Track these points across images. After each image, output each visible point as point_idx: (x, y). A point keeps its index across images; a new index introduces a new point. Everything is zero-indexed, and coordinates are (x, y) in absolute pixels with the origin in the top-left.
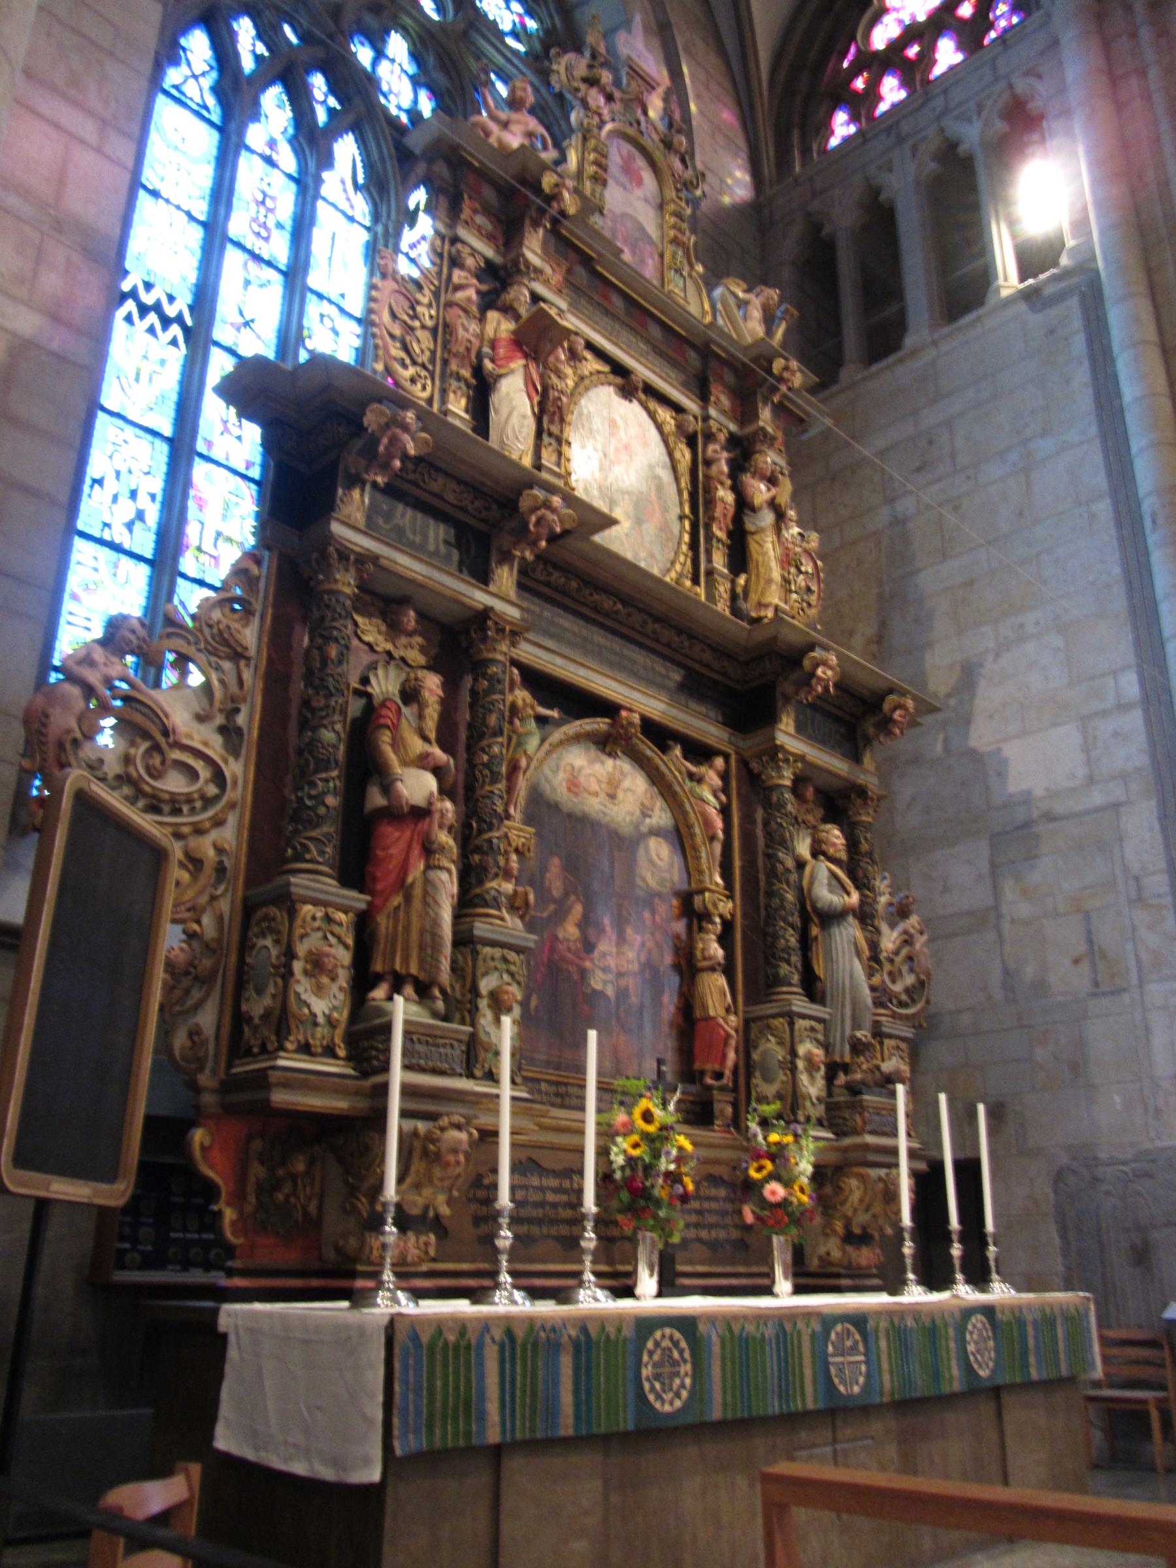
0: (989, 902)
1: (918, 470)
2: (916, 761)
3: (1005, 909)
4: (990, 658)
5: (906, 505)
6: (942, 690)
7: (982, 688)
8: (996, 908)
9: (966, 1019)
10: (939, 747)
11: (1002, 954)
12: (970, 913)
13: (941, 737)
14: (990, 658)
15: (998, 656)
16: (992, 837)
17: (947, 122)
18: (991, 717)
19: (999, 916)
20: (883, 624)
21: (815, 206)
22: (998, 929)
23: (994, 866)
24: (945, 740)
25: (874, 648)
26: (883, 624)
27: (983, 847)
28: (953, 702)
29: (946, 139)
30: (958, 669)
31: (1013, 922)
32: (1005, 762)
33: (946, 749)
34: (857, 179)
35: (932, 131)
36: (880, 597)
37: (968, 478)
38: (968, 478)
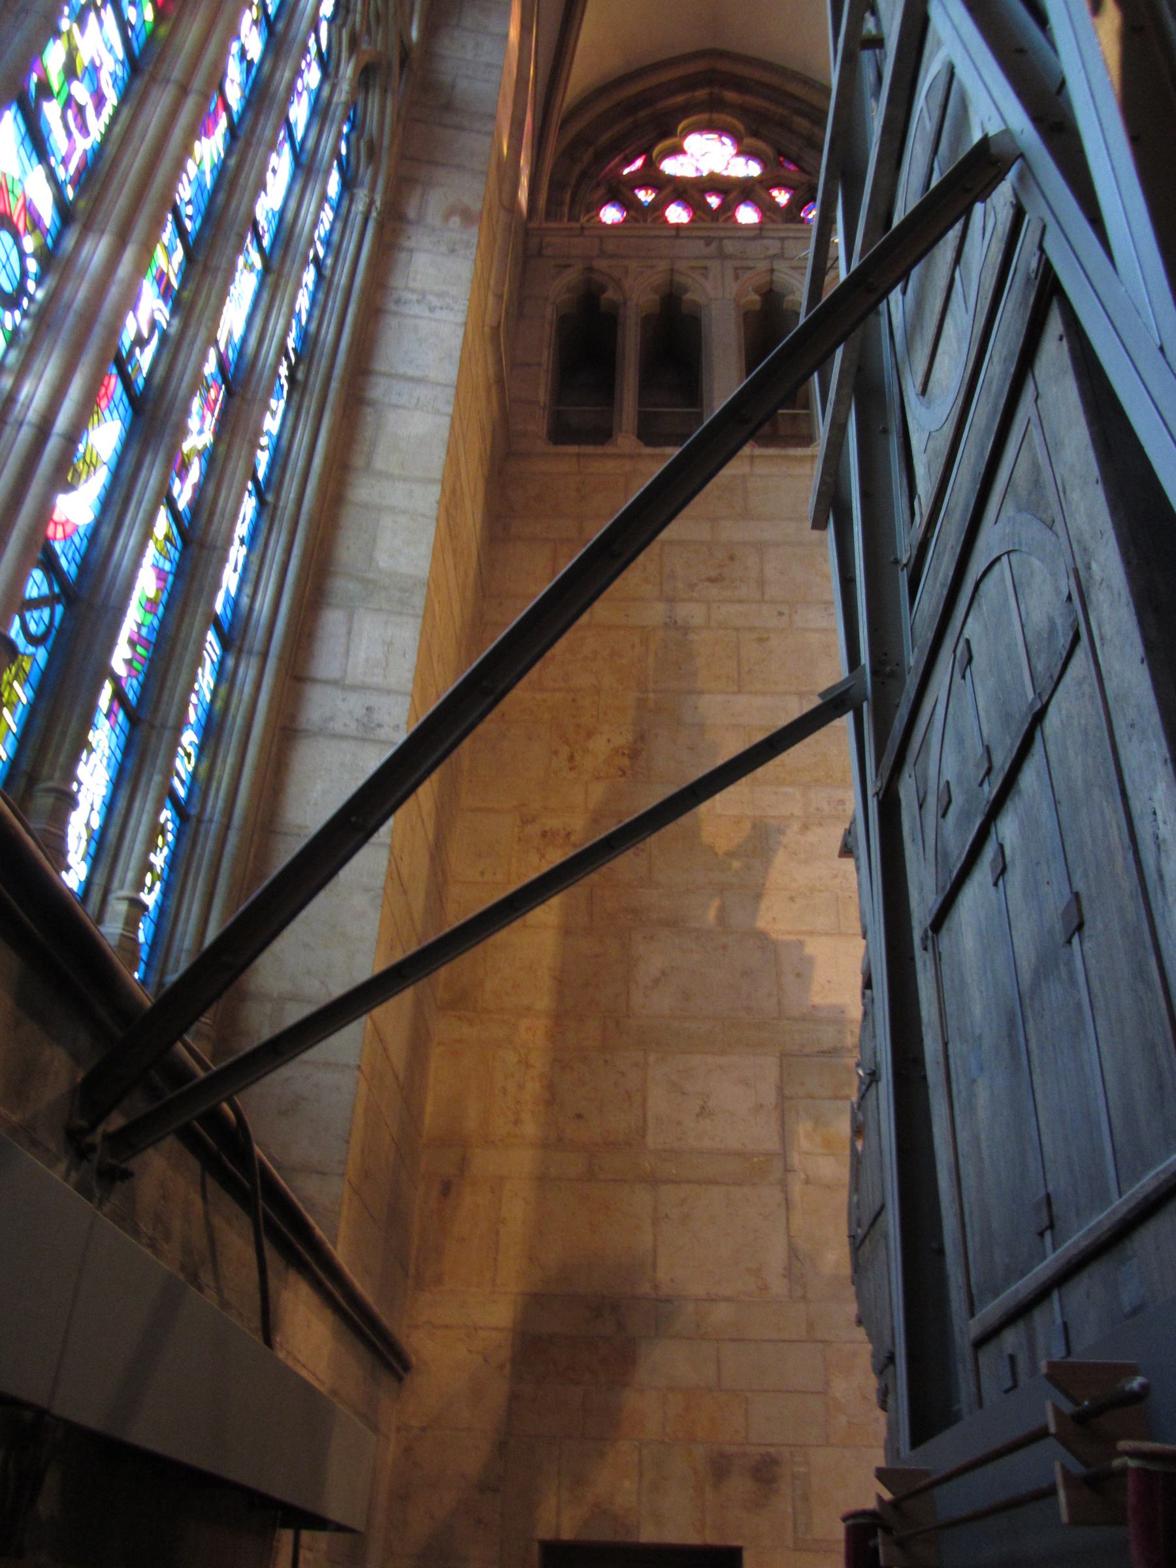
0: (773, 1144)
1: (711, 580)
2: (674, 923)
3: (795, 1159)
4: (796, 827)
5: (691, 612)
6: (722, 846)
7: (780, 858)
8: (784, 1155)
9: (722, 1313)
10: (712, 915)
11: (788, 1228)
12: (742, 1155)
13: (716, 903)
14: (796, 827)
15: (805, 827)
16: (783, 1055)
17: (780, 265)
18: (792, 899)
19: (788, 1170)
20: (641, 737)
21: (602, 264)
22: (784, 1185)
23: (782, 1096)
24: (722, 910)
25: (626, 762)
26: (641, 737)
27: (769, 1065)
28: (736, 864)
29: (772, 282)
30: (748, 825)
31: (807, 1181)
32: (809, 961)
33: (722, 918)
34: (663, 265)
35: (762, 266)
36: (641, 704)
37: (781, 614)
38: (781, 614)
